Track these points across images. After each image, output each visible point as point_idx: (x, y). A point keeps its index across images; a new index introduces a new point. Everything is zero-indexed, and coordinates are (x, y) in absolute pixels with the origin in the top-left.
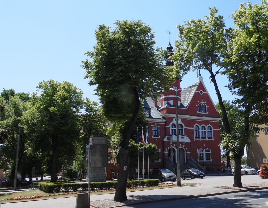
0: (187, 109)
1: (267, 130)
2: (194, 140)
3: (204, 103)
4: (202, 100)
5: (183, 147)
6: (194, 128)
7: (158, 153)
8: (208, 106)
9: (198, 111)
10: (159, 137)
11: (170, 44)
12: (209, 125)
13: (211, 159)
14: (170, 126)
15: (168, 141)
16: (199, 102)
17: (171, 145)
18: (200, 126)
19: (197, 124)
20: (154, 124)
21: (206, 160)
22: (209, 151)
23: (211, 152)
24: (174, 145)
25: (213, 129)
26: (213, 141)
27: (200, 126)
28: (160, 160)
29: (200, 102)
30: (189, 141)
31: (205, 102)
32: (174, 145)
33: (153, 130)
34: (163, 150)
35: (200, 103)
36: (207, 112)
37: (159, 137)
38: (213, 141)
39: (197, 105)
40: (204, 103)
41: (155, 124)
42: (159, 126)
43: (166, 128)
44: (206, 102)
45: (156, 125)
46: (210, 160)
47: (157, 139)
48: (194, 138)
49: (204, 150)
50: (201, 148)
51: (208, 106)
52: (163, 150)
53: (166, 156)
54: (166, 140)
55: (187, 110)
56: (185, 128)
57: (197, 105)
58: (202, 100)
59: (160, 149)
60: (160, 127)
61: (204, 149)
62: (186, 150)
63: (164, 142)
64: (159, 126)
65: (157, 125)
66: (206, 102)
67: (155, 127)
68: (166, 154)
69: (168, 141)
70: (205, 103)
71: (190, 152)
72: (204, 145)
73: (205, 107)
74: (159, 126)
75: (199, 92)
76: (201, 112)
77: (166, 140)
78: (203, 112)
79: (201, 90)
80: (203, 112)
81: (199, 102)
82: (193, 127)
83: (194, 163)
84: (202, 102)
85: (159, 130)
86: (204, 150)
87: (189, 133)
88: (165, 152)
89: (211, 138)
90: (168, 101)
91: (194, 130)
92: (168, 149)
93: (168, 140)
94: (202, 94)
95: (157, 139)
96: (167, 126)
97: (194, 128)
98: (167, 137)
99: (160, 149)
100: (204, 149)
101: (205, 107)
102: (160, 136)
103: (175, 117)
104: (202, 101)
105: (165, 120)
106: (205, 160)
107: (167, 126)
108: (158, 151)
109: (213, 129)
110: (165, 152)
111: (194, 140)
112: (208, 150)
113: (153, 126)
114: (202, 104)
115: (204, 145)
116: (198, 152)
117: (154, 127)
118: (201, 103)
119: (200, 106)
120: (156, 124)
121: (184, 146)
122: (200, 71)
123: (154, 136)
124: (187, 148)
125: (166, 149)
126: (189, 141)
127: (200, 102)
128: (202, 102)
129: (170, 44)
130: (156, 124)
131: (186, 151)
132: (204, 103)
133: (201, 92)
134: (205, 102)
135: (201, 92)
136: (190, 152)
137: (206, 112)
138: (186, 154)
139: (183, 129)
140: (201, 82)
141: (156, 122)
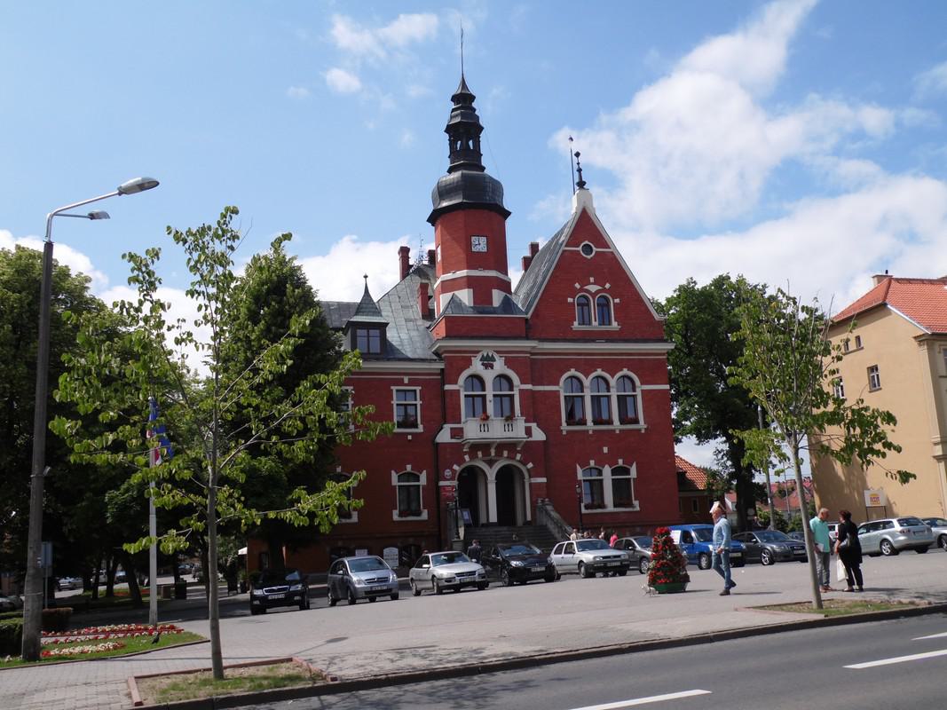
0: (529, 316)
1: (878, 375)
2: (564, 433)
4: (592, 280)
5: (519, 461)
6: (562, 389)
7: (419, 486)
8: (617, 301)
9: (576, 324)
10: (420, 429)
12: (625, 371)
13: (636, 503)
14: (460, 385)
15: (454, 441)
16: (577, 286)
17: (467, 457)
19: (573, 372)
20: (400, 382)
21: (615, 506)
22: (627, 472)
23: (633, 473)
24: (480, 454)
25: (640, 388)
26: (643, 431)
28: (425, 515)
30: (539, 435)
31: (603, 285)
32: (480, 454)
33: (395, 402)
34: (435, 477)
35: (581, 290)
36: (615, 325)
37: (420, 429)
38: (643, 431)
39: (570, 300)
41: (403, 379)
43: (444, 392)
44: (608, 286)
45: (406, 385)
46: (419, 513)
47: (410, 437)
48: (564, 424)
49: (607, 470)
50: (592, 463)
51: (617, 301)
52: (435, 477)
53: (448, 499)
54: (444, 436)
55: (530, 322)
56: (521, 391)
57: (570, 300)
58: (592, 280)
59: (425, 471)
61: (607, 466)
62: (528, 470)
63: (438, 443)
65: (411, 383)
66: (608, 286)
67: (405, 391)
68: (447, 489)
69: (454, 441)
70: (604, 290)
71: (544, 480)
72: (605, 450)
73: (604, 305)
74: (418, 389)
76: (590, 323)
77: (444, 436)
78: (595, 323)
79: (586, 242)
80: (595, 323)
81: (577, 286)
82: (557, 384)
83: (552, 519)
84: (593, 288)
85: (419, 402)
86: (607, 470)
87: (538, 408)
88: (442, 483)
89: (636, 421)
90: (456, 293)
92: (454, 471)
93: (452, 438)
94: (589, 257)
95: (410, 437)
96: (447, 387)
97: (562, 389)
98: (447, 427)
99: (425, 471)
100: (607, 466)
101: (604, 305)
103: (478, 352)
104: (590, 284)
105: (441, 366)
106: (610, 508)
107: (447, 387)
108: (418, 479)
109: (640, 388)
110: (442, 483)
111: (564, 433)
112: (409, 473)
113: (394, 388)
114: (594, 295)
115: (605, 450)
117: (397, 391)
118: (587, 291)
119: (584, 304)
120: (406, 381)
121: (518, 457)
123: (400, 425)
124: (530, 465)
125: (448, 473)
126: (539, 435)
128: (593, 288)
130: (406, 381)
131: (530, 477)
133: (588, 249)
134: (603, 285)
135: (588, 249)
136: (544, 480)
137: (610, 324)
138: (530, 484)
139: (516, 393)
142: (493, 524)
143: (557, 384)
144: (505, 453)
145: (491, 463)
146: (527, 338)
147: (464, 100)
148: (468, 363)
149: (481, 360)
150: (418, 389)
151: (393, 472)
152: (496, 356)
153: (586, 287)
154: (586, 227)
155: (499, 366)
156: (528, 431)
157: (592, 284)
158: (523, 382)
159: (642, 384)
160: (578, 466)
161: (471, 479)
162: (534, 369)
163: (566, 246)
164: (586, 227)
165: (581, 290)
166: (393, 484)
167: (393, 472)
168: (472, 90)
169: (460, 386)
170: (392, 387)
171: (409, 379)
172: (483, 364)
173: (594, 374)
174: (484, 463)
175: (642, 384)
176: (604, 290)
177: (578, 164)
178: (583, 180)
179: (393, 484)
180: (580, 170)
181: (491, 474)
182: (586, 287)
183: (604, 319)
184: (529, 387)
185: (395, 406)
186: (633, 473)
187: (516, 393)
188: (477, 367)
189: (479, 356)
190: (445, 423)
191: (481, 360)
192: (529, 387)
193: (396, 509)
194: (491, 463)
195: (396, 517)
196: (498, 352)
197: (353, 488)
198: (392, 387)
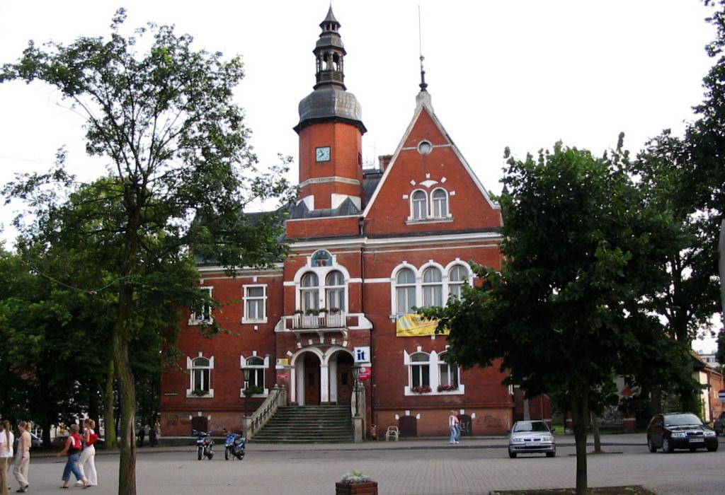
0: (365, 214)
3: (433, 187)
4: (428, 176)
5: (346, 347)
8: (453, 193)
11: (330, 11)
16: (413, 183)
18: (418, 269)
19: (405, 264)
20: (250, 281)
27: (418, 269)
29: (418, 182)
31: (439, 180)
33: (245, 298)
40: (437, 182)
41: (252, 279)
42: (266, 285)
44: (444, 180)
45: (255, 283)
47: (256, 328)
51: (453, 193)
54: (281, 328)
57: (405, 197)
58: (428, 176)
60: (266, 288)
61: (434, 353)
64: (266, 285)
66: (444, 180)
70: (440, 184)
74: (265, 286)
77: (281, 328)
81: (413, 183)
85: (265, 297)
91: (394, 285)
95: (256, 328)
96: (286, 284)
97: (393, 280)
100: (434, 353)
104: (426, 179)
107: (286, 284)
108: (262, 363)
113: (245, 286)
114: (429, 190)
116: (405, 363)
118: (424, 187)
120: (255, 280)
122: (425, 76)
128: (428, 184)
130: (255, 280)
132: (437, 182)
140: (424, 109)
142: (334, 403)
143: (389, 276)
144: (333, 341)
145: (324, 349)
146: (358, 236)
147: (330, 26)
150: (265, 286)
151: (242, 357)
153: (421, 184)
156: (354, 322)
157: (428, 179)
158: (352, 276)
160: (405, 353)
162: (360, 264)
163: (404, 147)
168: (338, 17)
170: (243, 286)
171: (258, 278)
173: (426, 265)
174: (319, 350)
176: (440, 184)
178: (426, 82)
180: (423, 73)
182: (421, 184)
184: (359, 280)
185: (245, 301)
186: (211, 366)
187: (346, 287)
190: (283, 315)
192: (359, 280)
193: (407, 385)
194: (324, 349)
195: (408, 391)
196: (331, 250)
198: (243, 286)
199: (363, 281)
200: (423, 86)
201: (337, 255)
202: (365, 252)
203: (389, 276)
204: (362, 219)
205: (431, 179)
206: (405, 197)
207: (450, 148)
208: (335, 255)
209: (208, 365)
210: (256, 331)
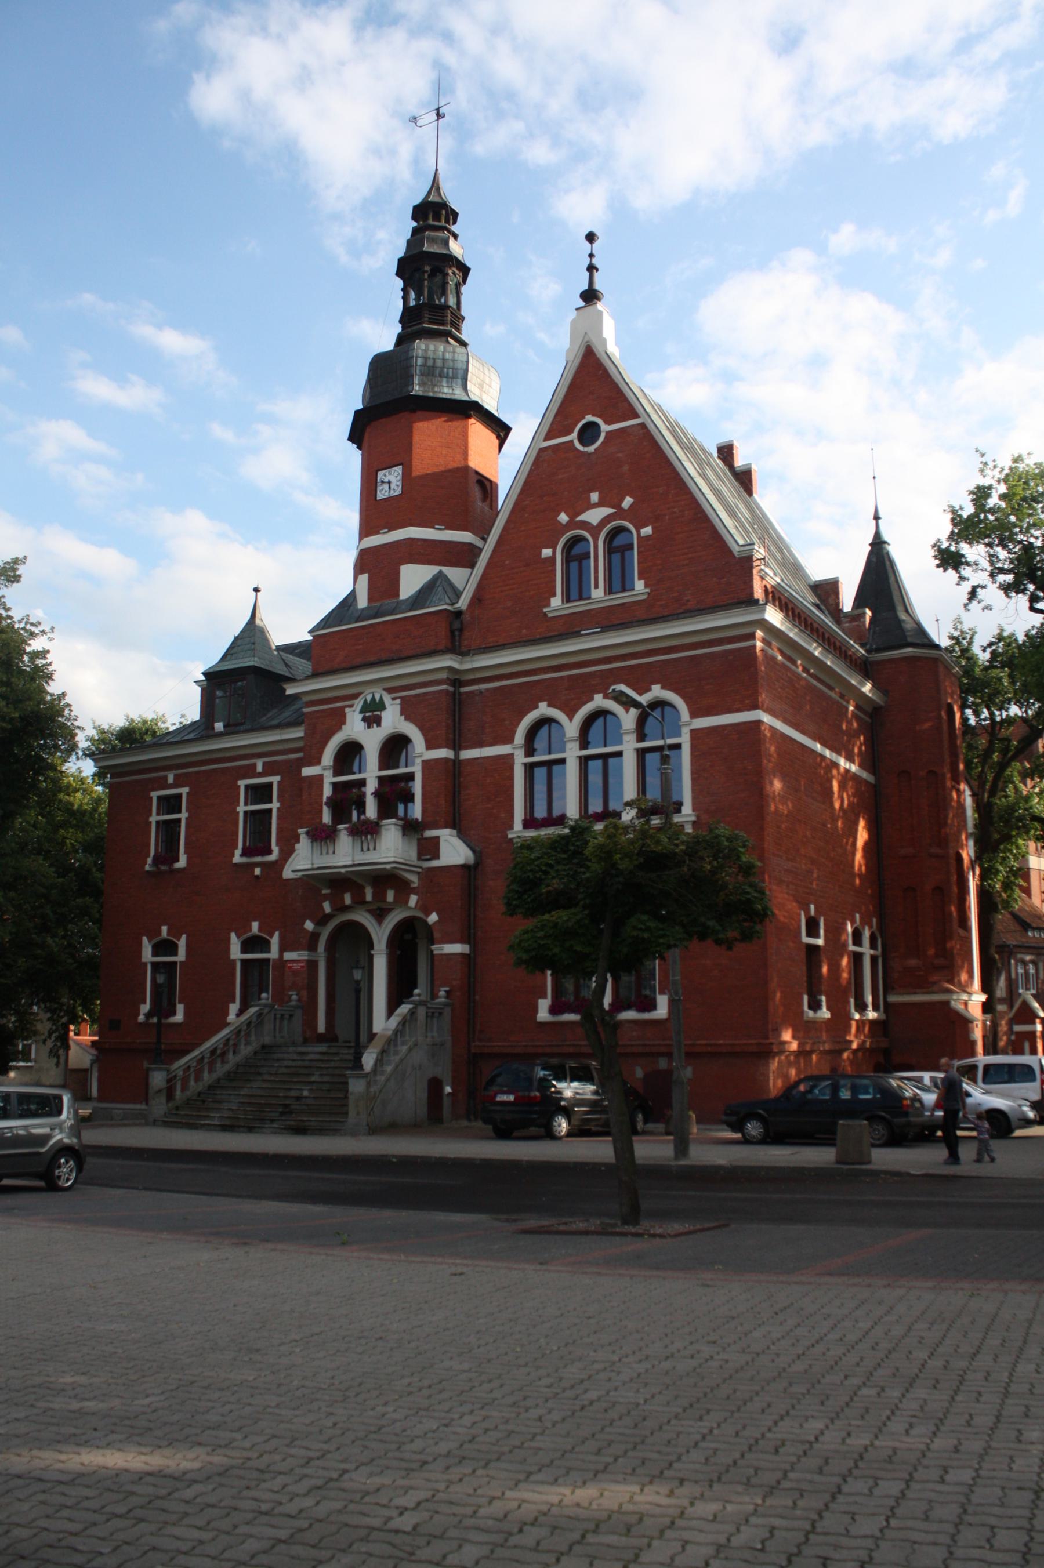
4: (595, 497)
8: (647, 531)
9: (556, 602)
11: (435, 184)
16: (563, 518)
18: (571, 720)
27: (571, 720)
29: (573, 515)
31: (617, 506)
36: (640, 585)
40: (613, 511)
44: (627, 502)
45: (260, 775)
47: (257, 871)
55: (467, 618)
56: (426, 764)
58: (595, 497)
65: (269, 770)
66: (627, 502)
70: (620, 513)
74: (275, 779)
75: (605, 428)
78: (598, 593)
80: (598, 593)
96: (307, 771)
97: (515, 750)
99: (277, 934)
101: (617, 544)
102: (277, 845)
103: (355, 696)
104: (592, 506)
107: (307, 771)
109: (688, 724)
113: (242, 783)
118: (585, 525)
119: (575, 554)
122: (596, 275)
127: (573, 515)
128: (594, 516)
129: (435, 184)
132: (613, 511)
133: (589, 433)
135: (589, 433)
141: (259, 756)
145: (380, 915)
148: (339, 719)
149: (361, 712)
151: (233, 936)
152: (387, 699)
153: (579, 518)
154: (592, 386)
155: (393, 720)
159: (694, 714)
161: (352, 942)
164: (592, 386)
165: (572, 524)
166: (232, 957)
167: (233, 935)
169: (325, 768)
171: (264, 764)
172: (364, 719)
174: (369, 916)
175: (694, 714)
176: (620, 513)
177: (591, 256)
178: (597, 286)
179: (232, 957)
181: (380, 935)
182: (582, 517)
183: (618, 581)
184: (443, 753)
188: (354, 727)
189: (359, 704)
191: (361, 712)
194: (380, 915)
196: (390, 690)
197: (181, 962)
199: (457, 755)
200: (590, 296)
201: (402, 698)
202: (463, 690)
203: (509, 740)
204: (458, 614)
205: (600, 504)
206: (546, 552)
207: (643, 426)
208: (398, 701)
209: (176, 954)
210: (257, 876)
